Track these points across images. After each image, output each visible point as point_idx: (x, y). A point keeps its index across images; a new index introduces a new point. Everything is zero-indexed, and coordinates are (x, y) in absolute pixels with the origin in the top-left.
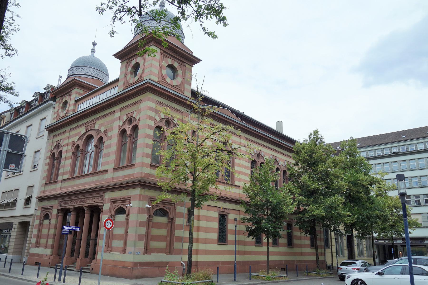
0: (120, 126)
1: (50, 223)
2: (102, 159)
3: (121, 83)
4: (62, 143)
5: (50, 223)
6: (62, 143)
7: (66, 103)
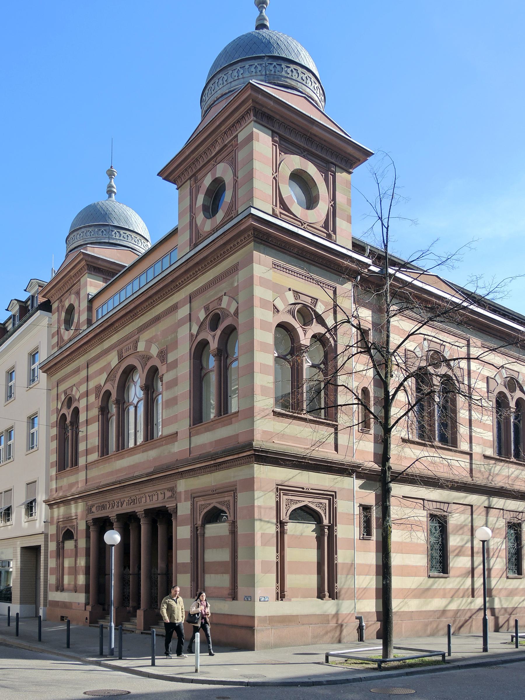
1: (76, 547)
2: (161, 413)
3: (184, 238)
4: (76, 393)
5: (76, 547)
7: (71, 310)
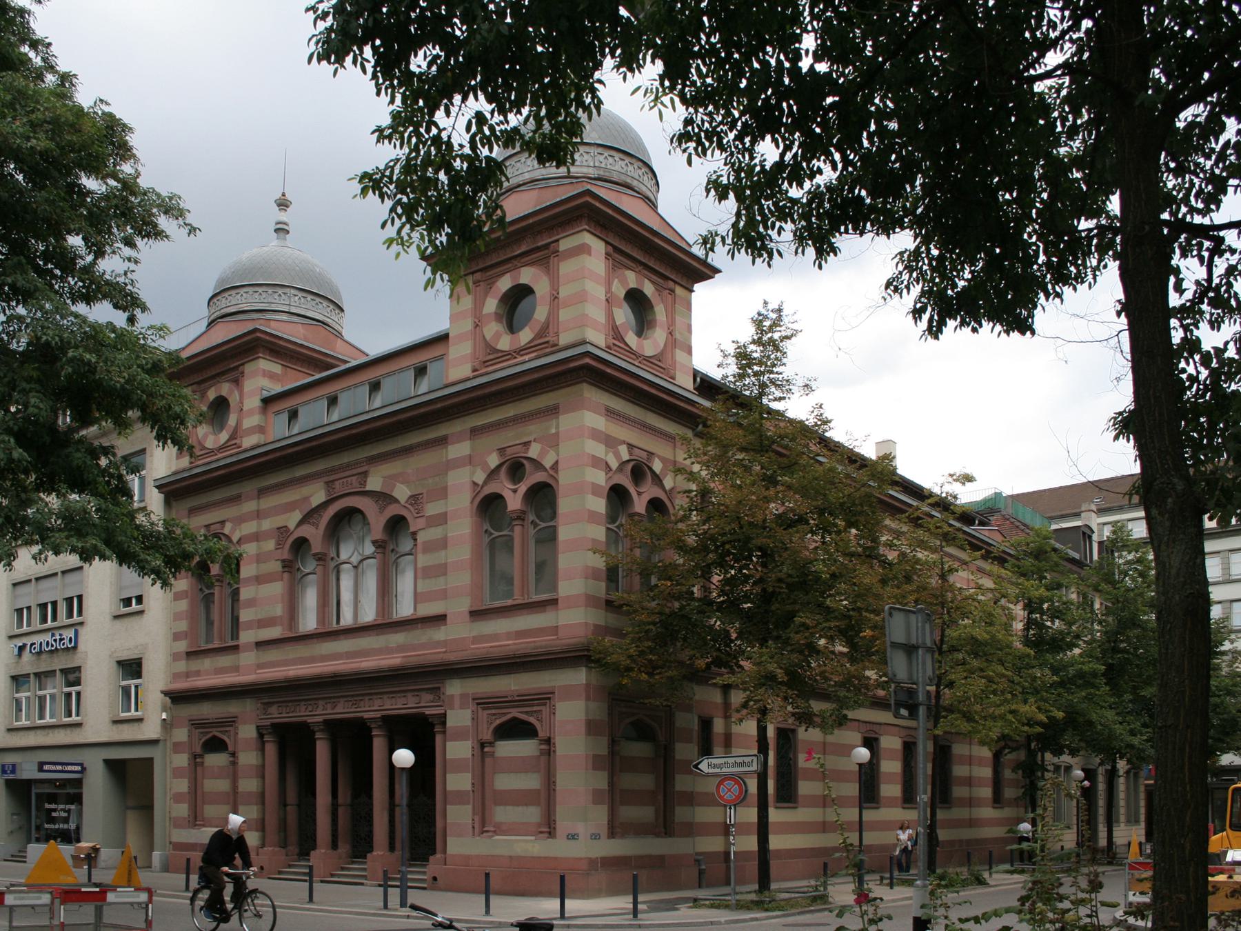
0: (475, 484)
4: (233, 530)
6: (233, 530)
